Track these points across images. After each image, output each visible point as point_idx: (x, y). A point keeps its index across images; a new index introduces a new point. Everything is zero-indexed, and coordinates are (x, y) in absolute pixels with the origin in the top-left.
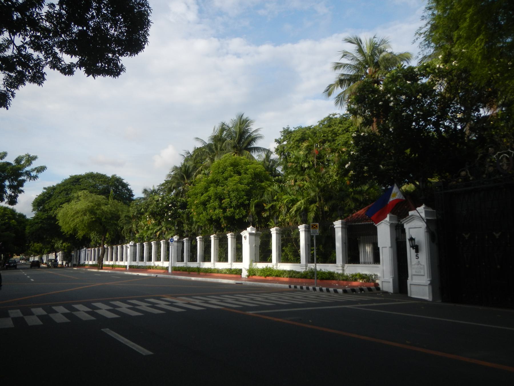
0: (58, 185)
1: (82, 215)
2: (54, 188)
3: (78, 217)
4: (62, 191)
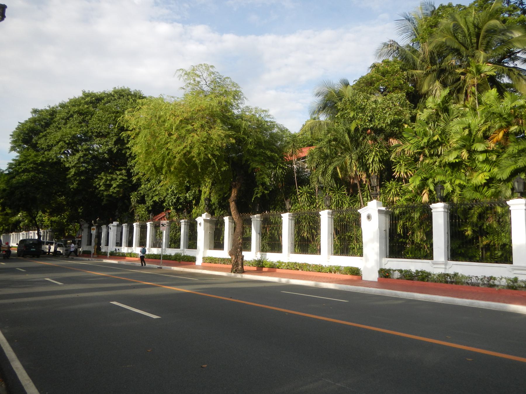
0: (63, 106)
1: (202, 126)
2: (53, 113)
3: (194, 131)
4: (72, 116)
